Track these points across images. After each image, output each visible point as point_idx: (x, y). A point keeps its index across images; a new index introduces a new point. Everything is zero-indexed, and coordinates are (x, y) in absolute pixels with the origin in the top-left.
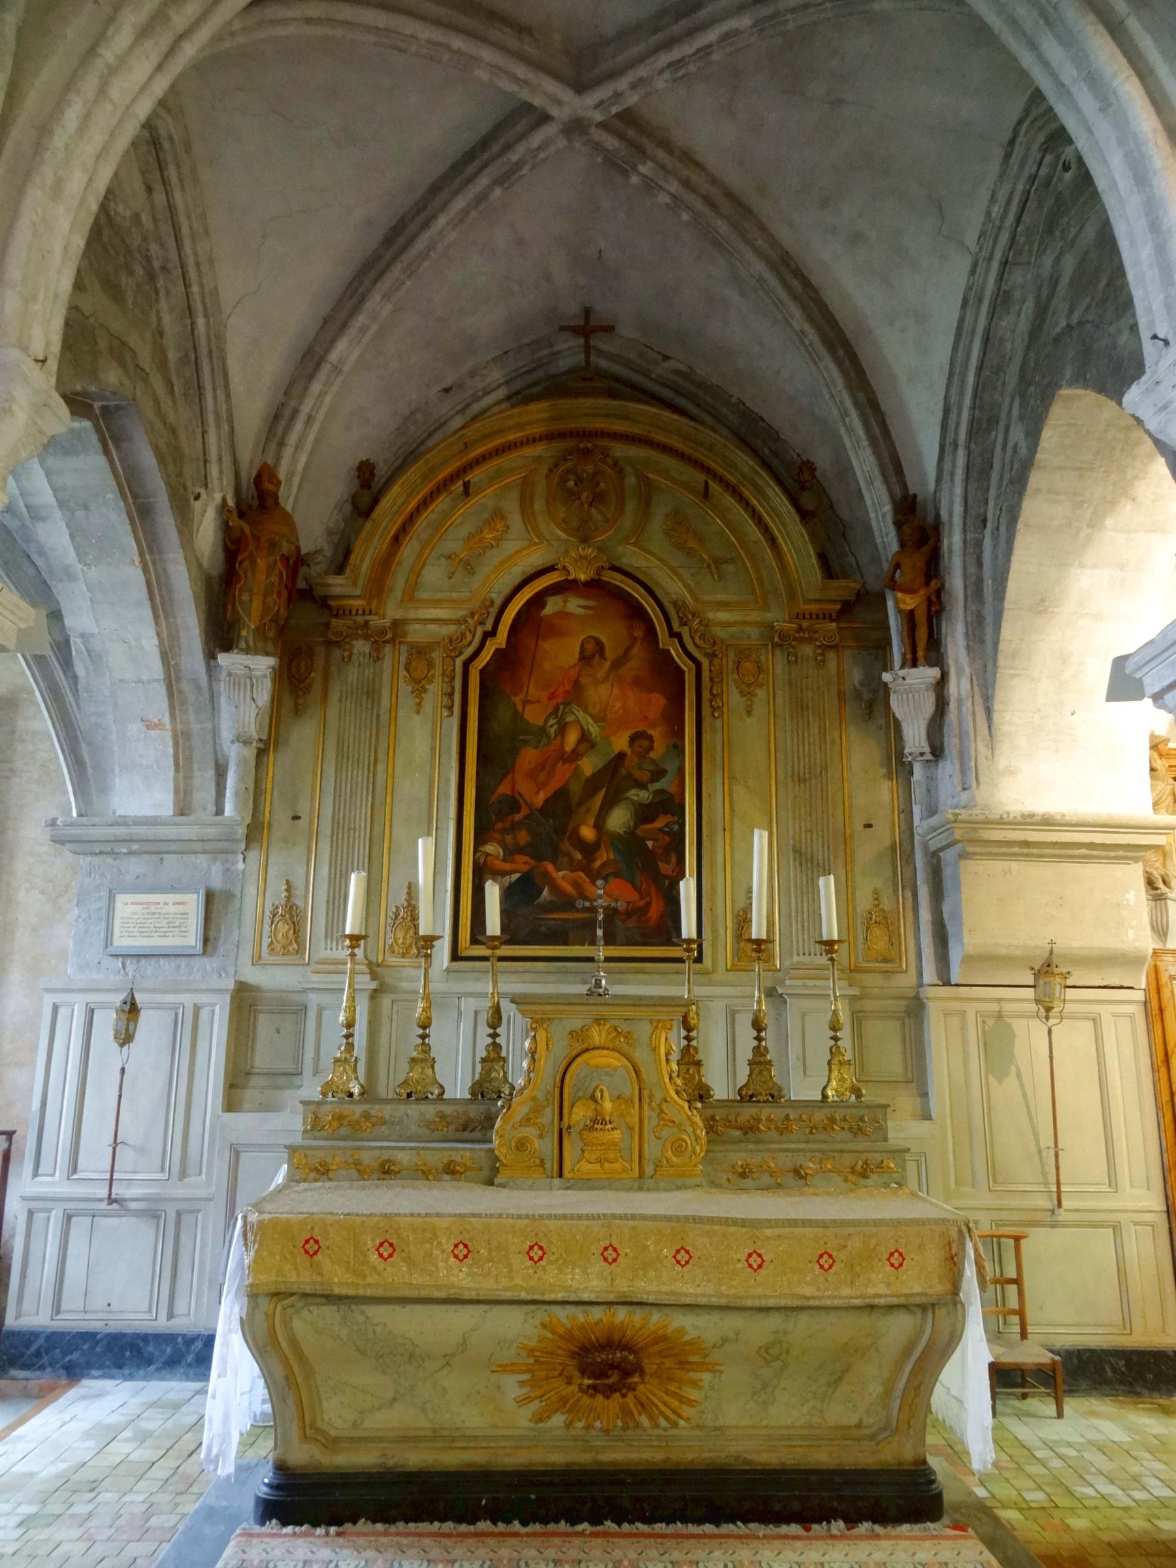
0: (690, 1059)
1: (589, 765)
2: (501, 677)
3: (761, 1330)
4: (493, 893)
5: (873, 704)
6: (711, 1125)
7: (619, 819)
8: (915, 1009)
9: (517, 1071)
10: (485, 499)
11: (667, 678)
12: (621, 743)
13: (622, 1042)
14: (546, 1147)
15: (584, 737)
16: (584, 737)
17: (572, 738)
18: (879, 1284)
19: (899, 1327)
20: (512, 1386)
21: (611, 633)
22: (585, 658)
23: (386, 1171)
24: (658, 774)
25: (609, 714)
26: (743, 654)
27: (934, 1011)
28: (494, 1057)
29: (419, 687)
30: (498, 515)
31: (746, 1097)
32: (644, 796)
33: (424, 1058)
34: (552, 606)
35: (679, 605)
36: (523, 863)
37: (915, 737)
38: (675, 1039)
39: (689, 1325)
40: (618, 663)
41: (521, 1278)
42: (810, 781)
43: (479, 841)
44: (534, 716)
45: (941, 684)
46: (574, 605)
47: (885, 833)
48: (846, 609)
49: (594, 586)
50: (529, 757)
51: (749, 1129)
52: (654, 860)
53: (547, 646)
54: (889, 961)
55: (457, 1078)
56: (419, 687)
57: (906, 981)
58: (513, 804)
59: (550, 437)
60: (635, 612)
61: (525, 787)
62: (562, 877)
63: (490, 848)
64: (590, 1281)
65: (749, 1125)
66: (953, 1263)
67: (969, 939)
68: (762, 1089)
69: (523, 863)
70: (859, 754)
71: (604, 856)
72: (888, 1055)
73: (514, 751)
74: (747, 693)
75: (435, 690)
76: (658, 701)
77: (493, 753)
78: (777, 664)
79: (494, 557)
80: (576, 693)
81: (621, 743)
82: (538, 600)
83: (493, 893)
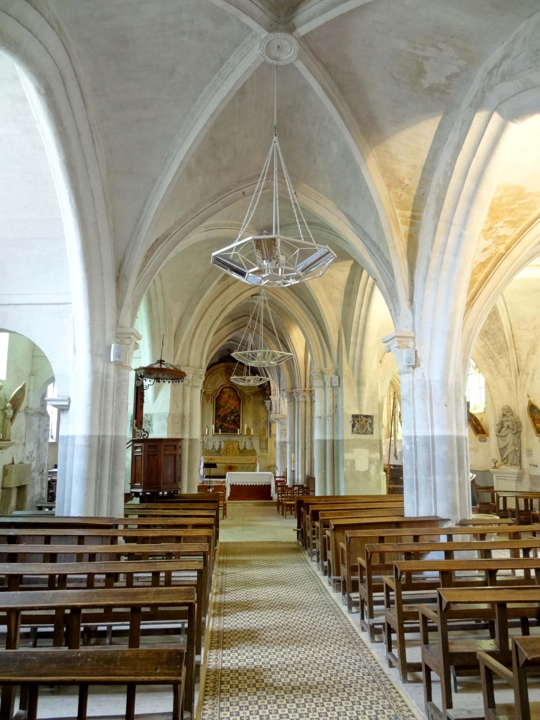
0: (238, 446)
1: (229, 411)
2: (218, 399)
3: (242, 465)
4: (220, 430)
5: (264, 403)
6: (240, 452)
7: (232, 418)
8: (267, 441)
9: (223, 447)
10: (216, 375)
11: (239, 399)
12: (233, 408)
13: (232, 444)
14: (225, 453)
15: (228, 407)
16: (228, 407)
17: (227, 407)
18: (251, 462)
19: (252, 465)
20: (223, 470)
21: (232, 393)
22: (229, 397)
23: (211, 455)
24: (237, 412)
25: (232, 404)
26: (248, 396)
27: (269, 441)
28: (220, 446)
29: (208, 400)
30: (218, 377)
31: (244, 449)
32: (236, 415)
33: (214, 446)
34: (225, 390)
35: (241, 390)
36: (221, 423)
37: (268, 409)
38: (237, 444)
39: (237, 465)
40: (233, 397)
41: (224, 461)
42: (256, 413)
43: (216, 420)
44: (222, 404)
45: (271, 403)
46: (227, 390)
47: (265, 419)
48: (261, 391)
49: (230, 387)
50: (221, 410)
51: (244, 452)
52: (236, 423)
53: (224, 395)
54: (264, 435)
55: (217, 448)
56: (208, 400)
57: (266, 437)
58: (219, 415)
59: (224, 366)
60: (235, 391)
61: (221, 414)
62: (226, 425)
63: (217, 421)
64: (229, 462)
65: (243, 452)
66: (256, 461)
67: (272, 433)
68: (245, 448)
69: (221, 423)
70: (262, 409)
71: (230, 422)
72: (264, 446)
73: (220, 409)
74: (249, 402)
75: (210, 401)
76: (238, 402)
77: (217, 409)
78: (252, 397)
79: (217, 383)
80: (227, 402)
81: (233, 408)
82: (223, 389)
83: (220, 430)
